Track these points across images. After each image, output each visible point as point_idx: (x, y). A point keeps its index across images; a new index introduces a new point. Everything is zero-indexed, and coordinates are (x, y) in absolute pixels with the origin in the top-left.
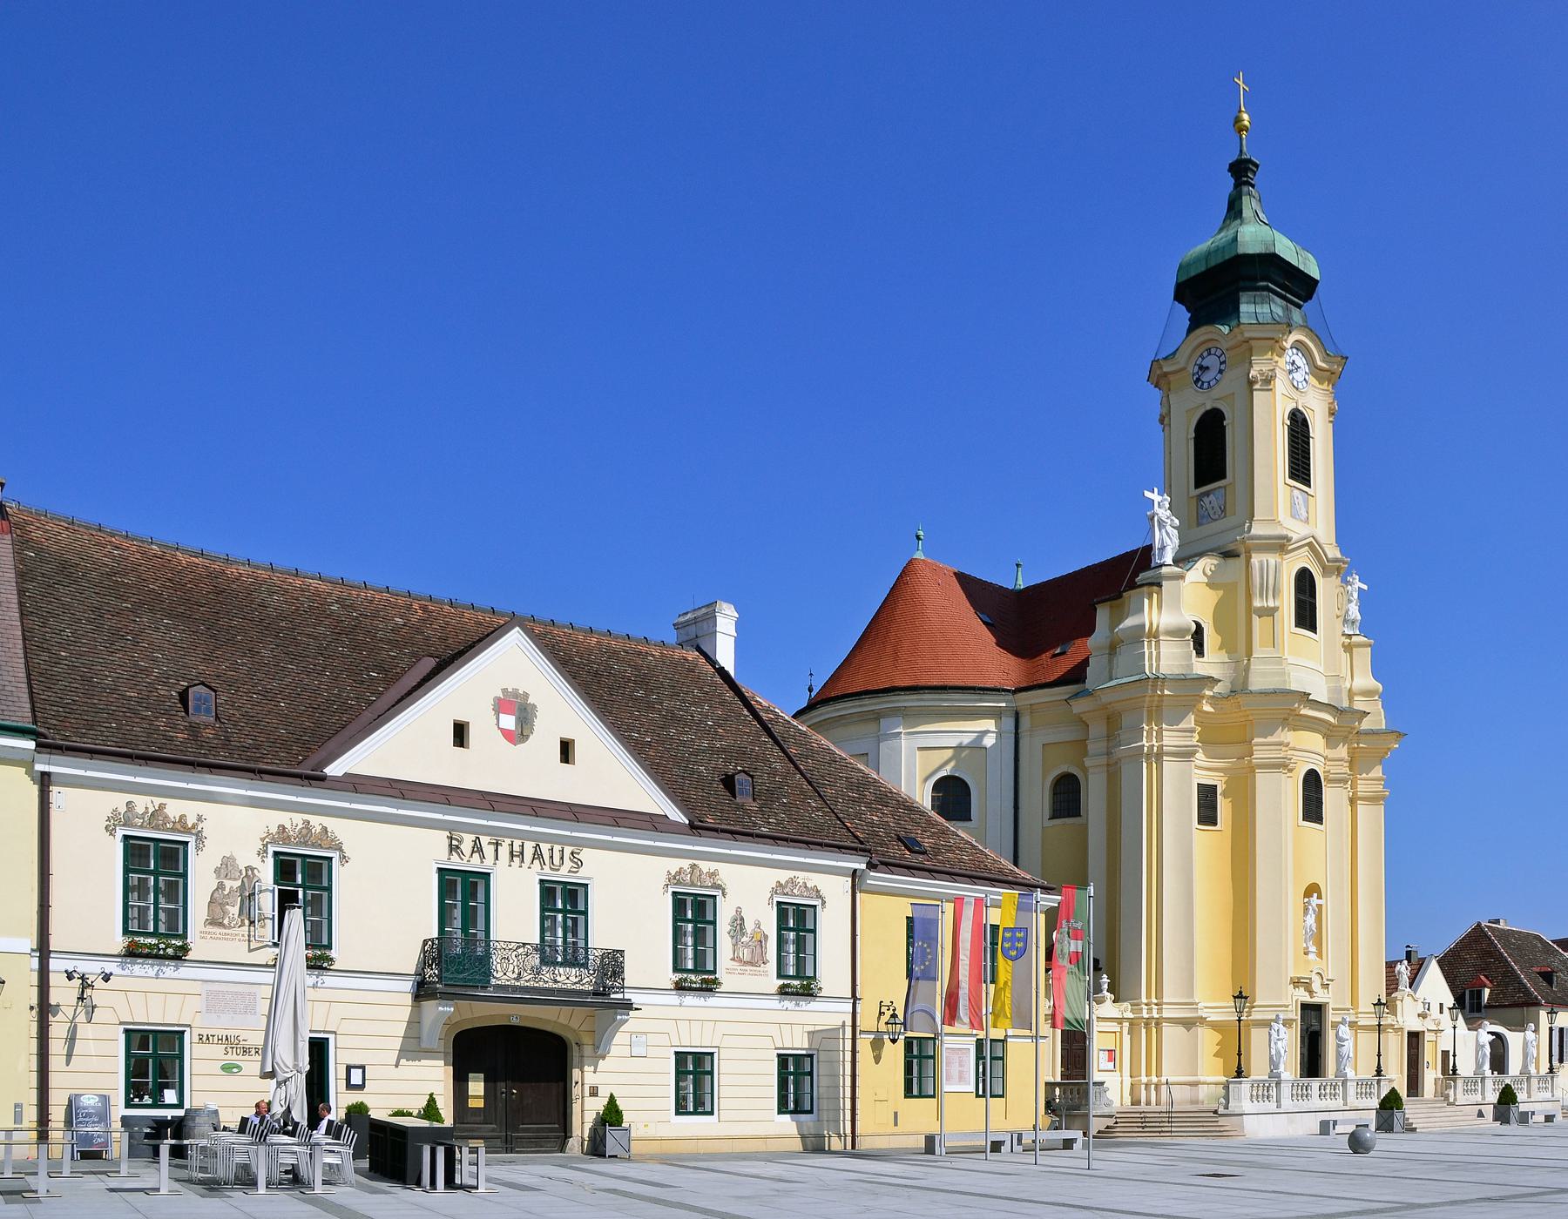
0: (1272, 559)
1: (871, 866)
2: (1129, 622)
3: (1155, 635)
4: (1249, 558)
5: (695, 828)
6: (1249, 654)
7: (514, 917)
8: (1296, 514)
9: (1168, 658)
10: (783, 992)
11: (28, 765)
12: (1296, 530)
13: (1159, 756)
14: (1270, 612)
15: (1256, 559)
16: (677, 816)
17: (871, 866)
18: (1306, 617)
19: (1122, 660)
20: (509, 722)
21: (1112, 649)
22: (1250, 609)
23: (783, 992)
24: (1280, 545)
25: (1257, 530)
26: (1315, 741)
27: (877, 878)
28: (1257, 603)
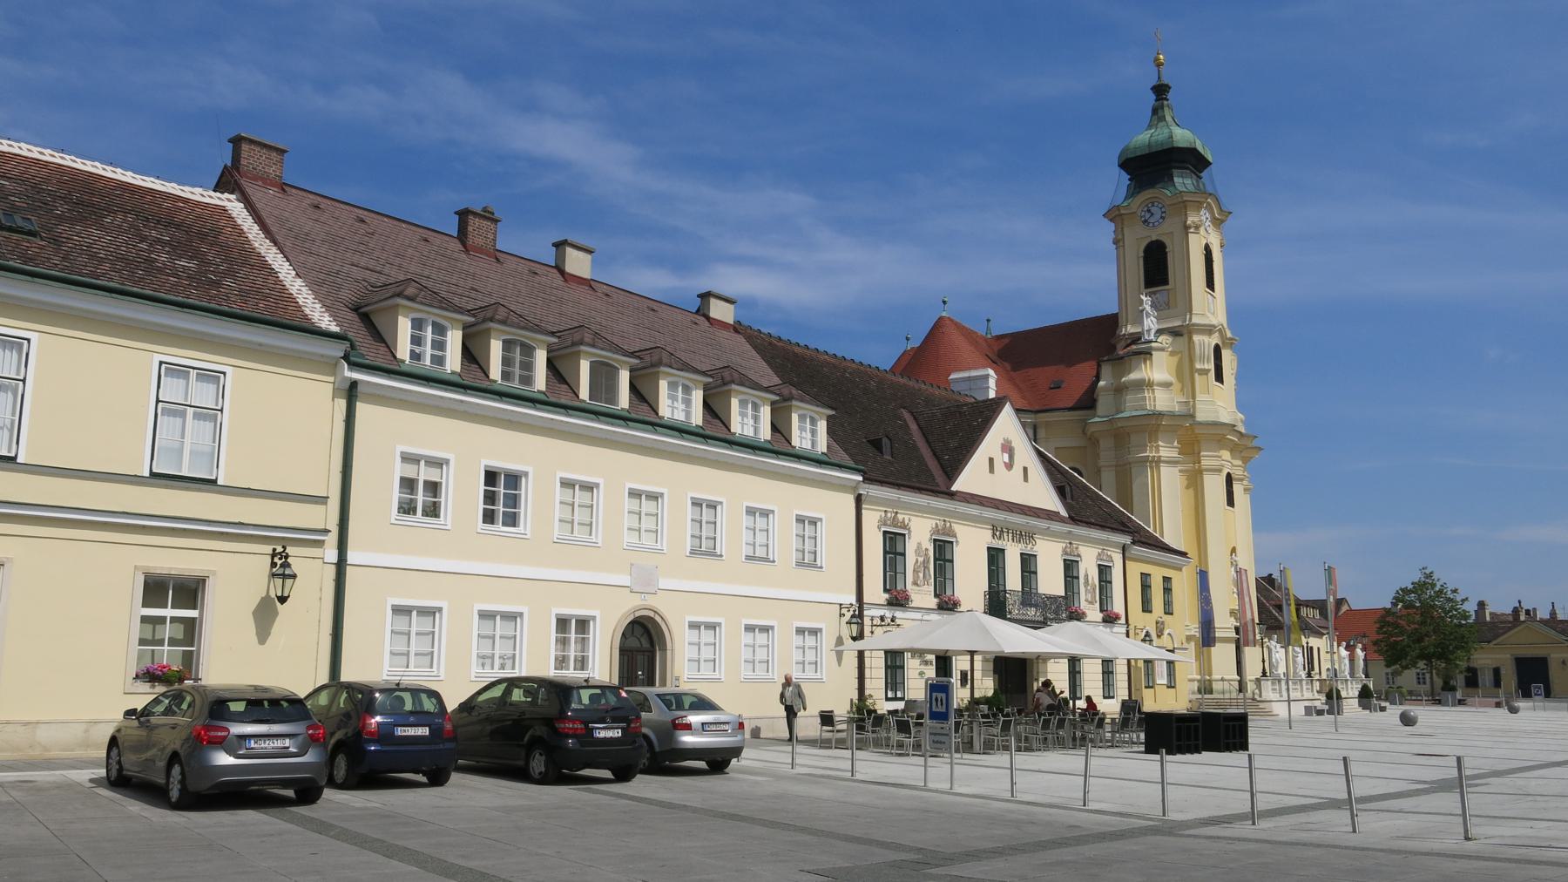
0: (1205, 338)
1: (1134, 543)
2: (1134, 376)
3: (1150, 384)
4: (1190, 338)
5: (1074, 519)
6: (1194, 397)
7: (1013, 580)
8: (1210, 308)
9: (1162, 401)
10: (1104, 621)
11: (854, 488)
12: (1214, 322)
13: (1158, 462)
14: (1205, 372)
15: (1196, 338)
16: (1064, 513)
17: (1134, 543)
18: (1219, 377)
19: (1130, 399)
20: (1006, 457)
21: (1120, 390)
22: (1192, 370)
23: (1104, 621)
24: (1209, 330)
25: (1195, 320)
26: (1226, 454)
27: (1138, 550)
28: (1198, 366)
